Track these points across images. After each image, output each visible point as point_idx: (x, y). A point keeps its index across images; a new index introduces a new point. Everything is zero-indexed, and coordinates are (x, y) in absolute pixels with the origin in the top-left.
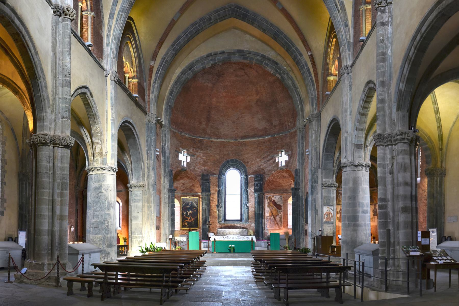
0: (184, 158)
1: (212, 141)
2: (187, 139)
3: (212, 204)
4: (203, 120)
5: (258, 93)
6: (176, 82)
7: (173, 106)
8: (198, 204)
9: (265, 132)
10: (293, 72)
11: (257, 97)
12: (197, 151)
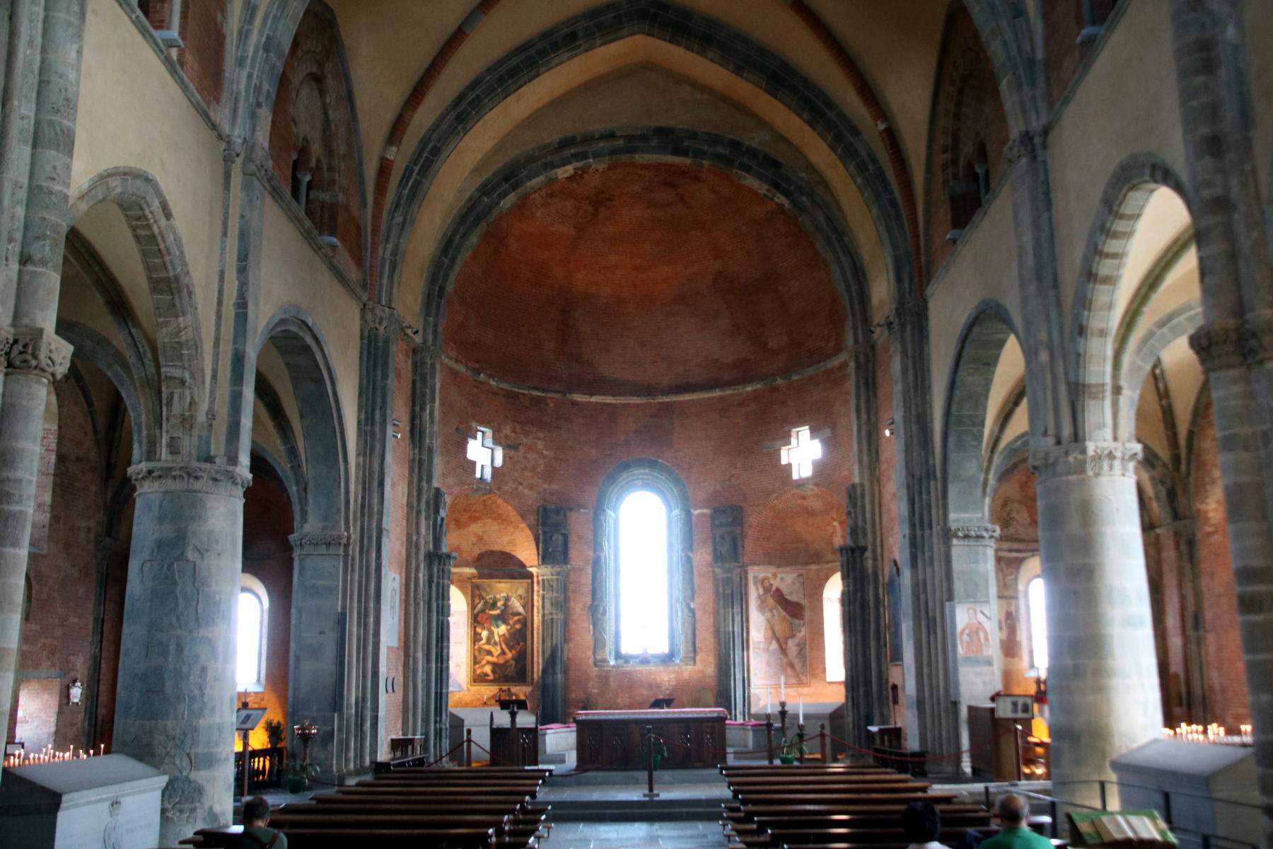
0: (483, 453)
1: (575, 404)
2: (495, 394)
3: (572, 604)
8: (528, 603)
9: (743, 372)
12: (527, 434)
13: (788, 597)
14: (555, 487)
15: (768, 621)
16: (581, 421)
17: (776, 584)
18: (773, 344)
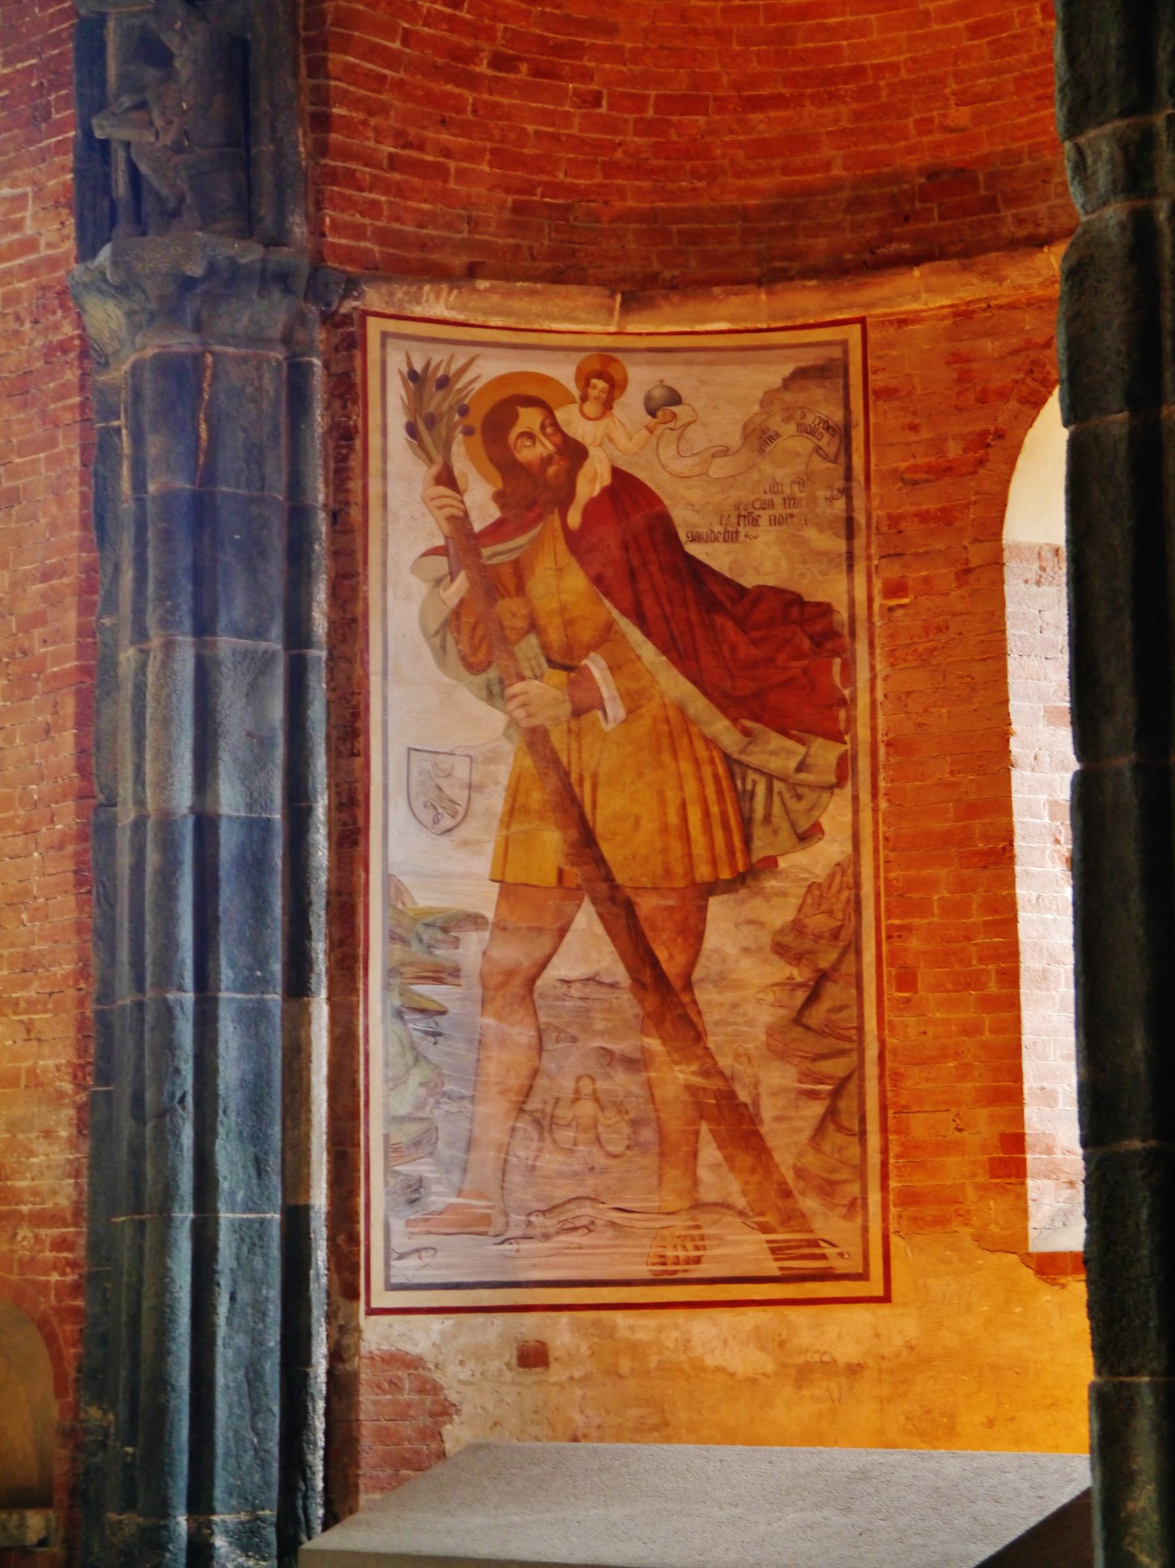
13: (714, 556)
15: (536, 739)
17: (612, 441)
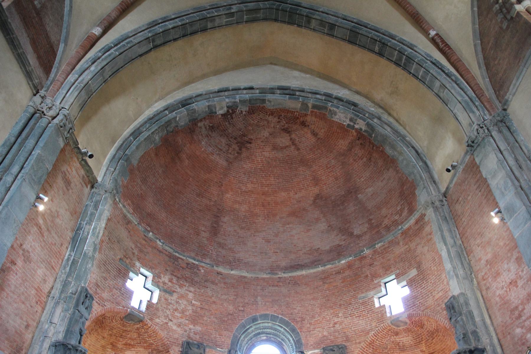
1: (219, 273)
2: (160, 252)
4: (203, 229)
5: (316, 181)
6: (151, 120)
7: (135, 162)
10: (390, 114)
11: (315, 190)
12: (181, 286)
14: (198, 328)
16: (222, 285)
18: (357, 232)
